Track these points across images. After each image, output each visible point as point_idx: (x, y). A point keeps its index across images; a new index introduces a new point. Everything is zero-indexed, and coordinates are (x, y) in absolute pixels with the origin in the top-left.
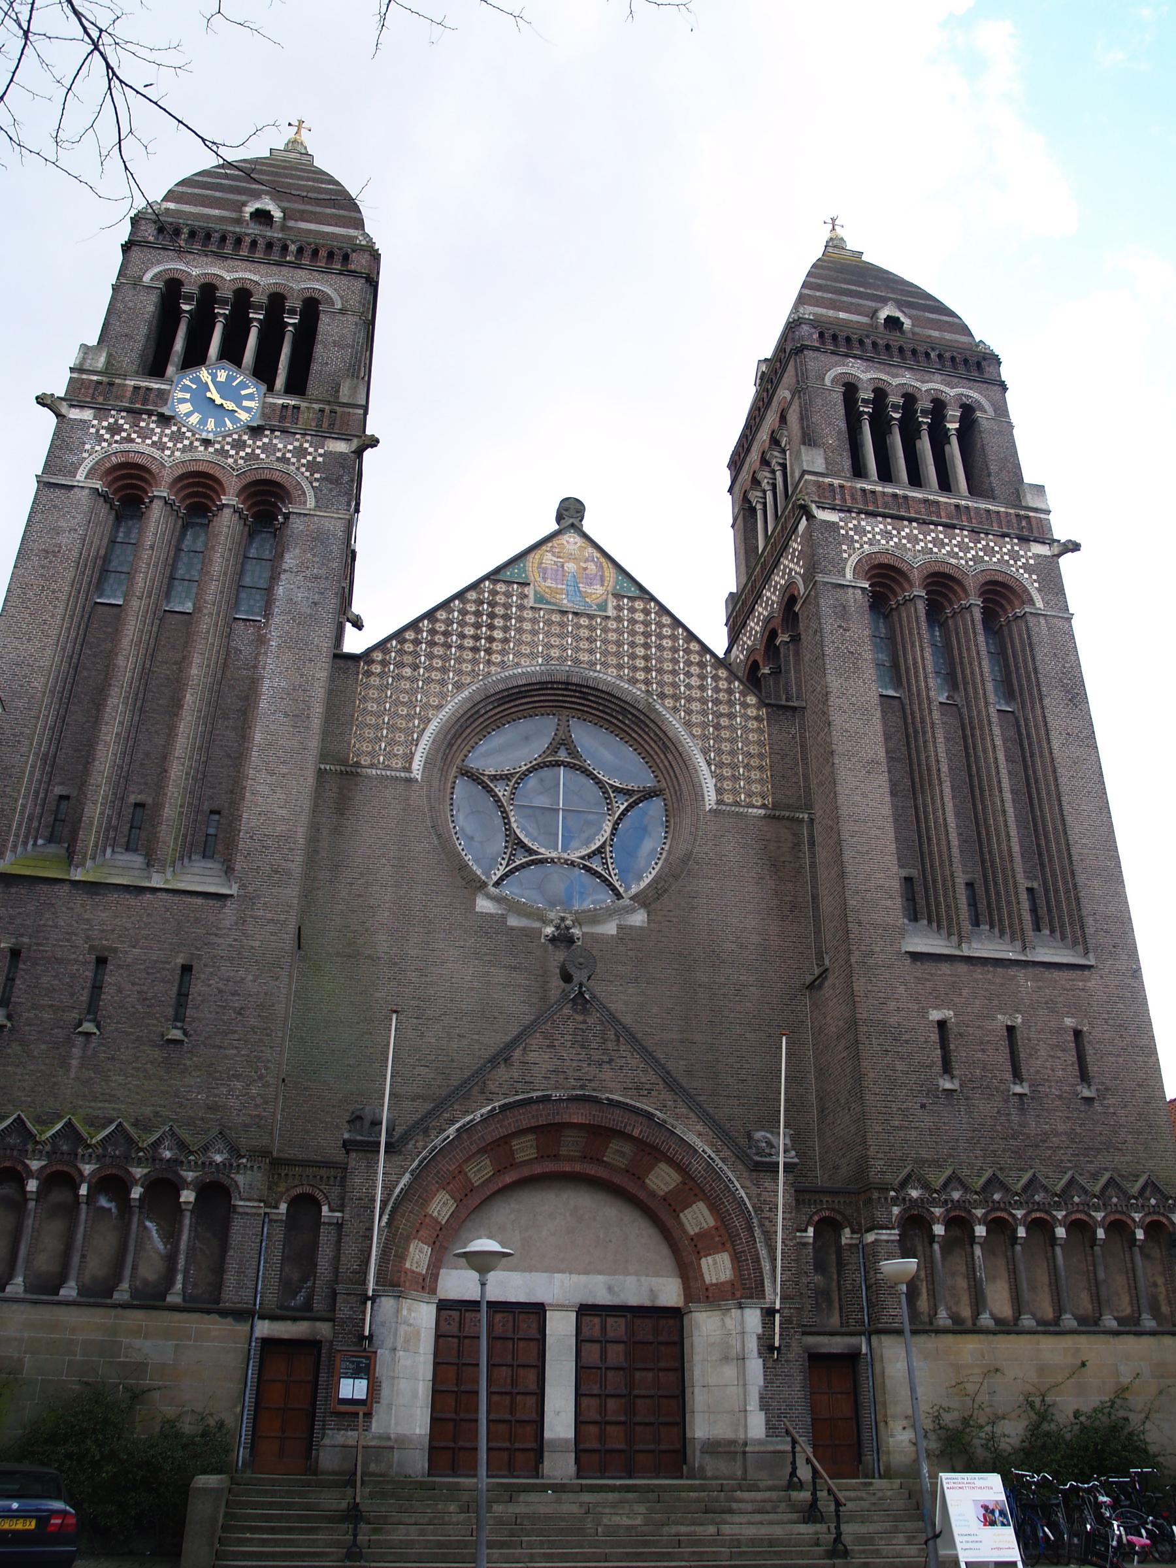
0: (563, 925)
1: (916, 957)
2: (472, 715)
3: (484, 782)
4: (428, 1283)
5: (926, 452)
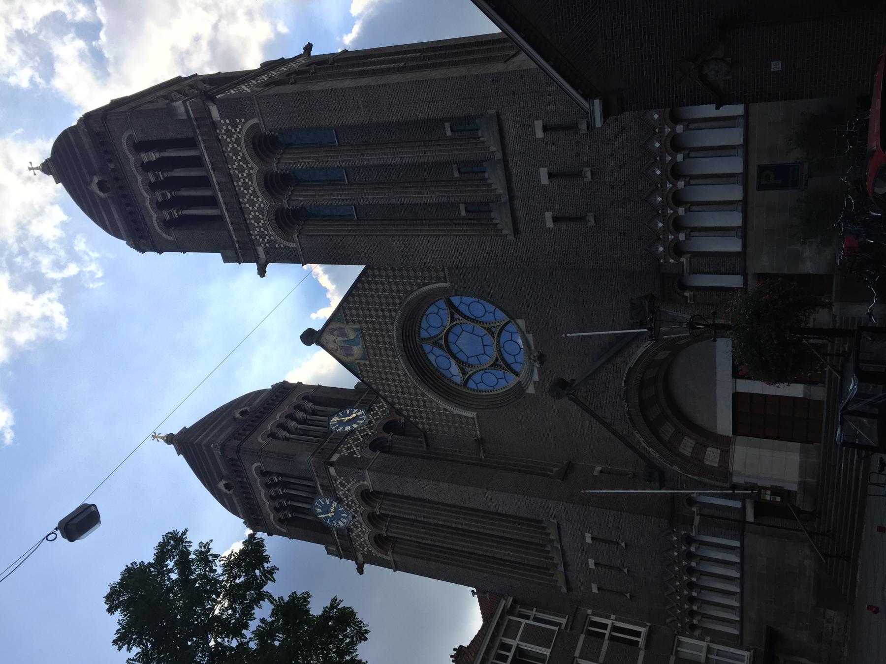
0: (533, 359)
1: (516, 231)
2: (435, 387)
3: (467, 378)
4: (724, 444)
5: (197, 211)
